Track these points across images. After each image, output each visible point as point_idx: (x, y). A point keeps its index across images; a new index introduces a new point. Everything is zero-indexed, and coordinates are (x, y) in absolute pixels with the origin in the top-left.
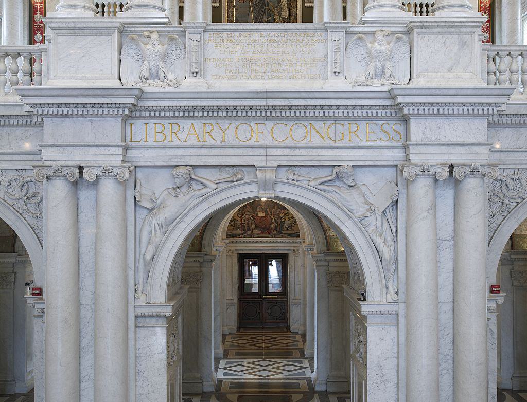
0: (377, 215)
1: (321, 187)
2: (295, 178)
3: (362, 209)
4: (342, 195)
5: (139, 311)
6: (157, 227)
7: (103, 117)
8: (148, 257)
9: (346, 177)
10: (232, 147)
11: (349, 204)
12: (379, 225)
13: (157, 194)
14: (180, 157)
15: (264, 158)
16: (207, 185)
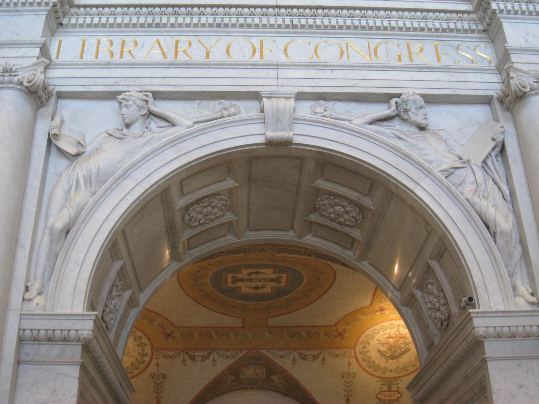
0: (473, 167)
1: (373, 127)
2: (325, 114)
3: (446, 160)
4: (409, 140)
5: (28, 324)
6: (82, 181)
7: (18, 11)
8: (59, 224)
9: (413, 110)
10: (220, 65)
11: (423, 152)
12: (480, 180)
13: (88, 140)
14: (133, 79)
15: (274, 82)
16: (174, 121)
